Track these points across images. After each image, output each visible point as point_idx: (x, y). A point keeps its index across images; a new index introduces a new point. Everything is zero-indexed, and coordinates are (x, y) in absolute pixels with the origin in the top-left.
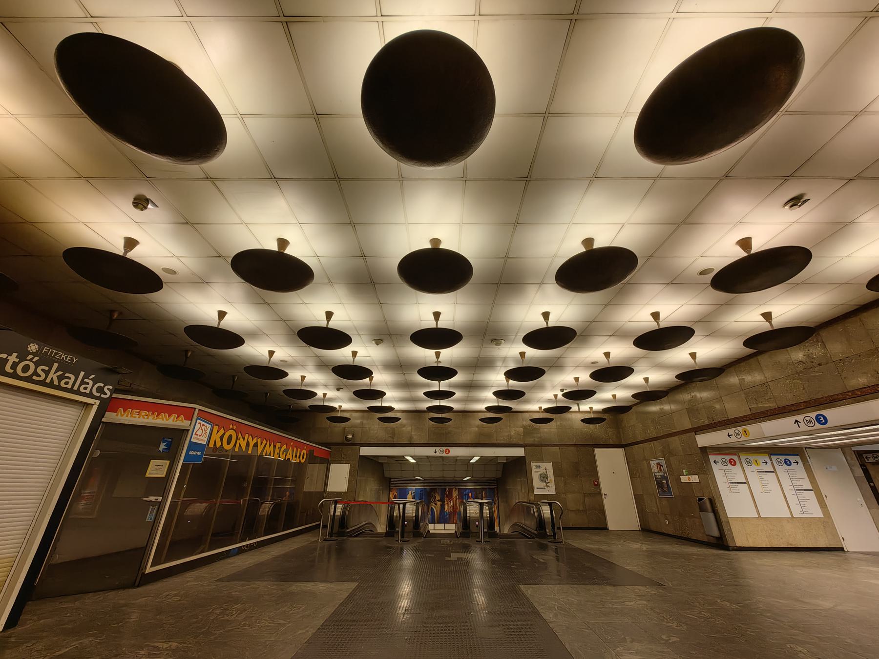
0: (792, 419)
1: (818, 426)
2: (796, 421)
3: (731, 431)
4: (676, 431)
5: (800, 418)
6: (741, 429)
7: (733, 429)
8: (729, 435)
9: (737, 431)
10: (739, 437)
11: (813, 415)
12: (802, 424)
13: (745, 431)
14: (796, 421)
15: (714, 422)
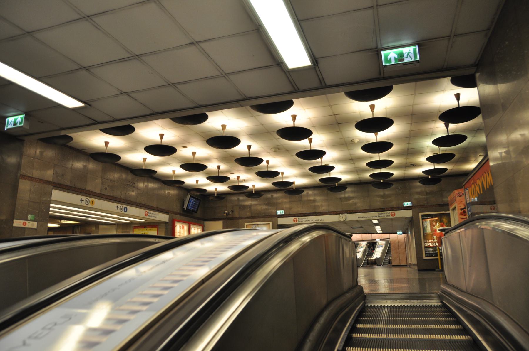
0: (116, 205)
1: (123, 212)
2: (117, 207)
3: (84, 198)
4: (31, 176)
5: (119, 205)
6: (91, 199)
7: (86, 198)
8: (81, 200)
9: (87, 200)
10: (87, 203)
11: (124, 206)
12: (119, 209)
13: (92, 202)
14: (117, 207)
15: (74, 186)
